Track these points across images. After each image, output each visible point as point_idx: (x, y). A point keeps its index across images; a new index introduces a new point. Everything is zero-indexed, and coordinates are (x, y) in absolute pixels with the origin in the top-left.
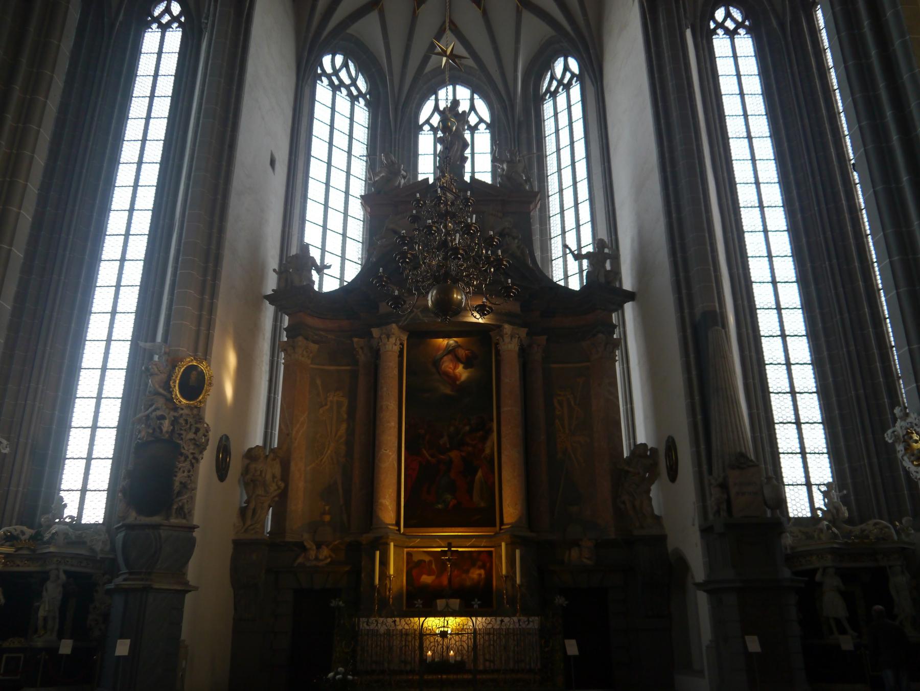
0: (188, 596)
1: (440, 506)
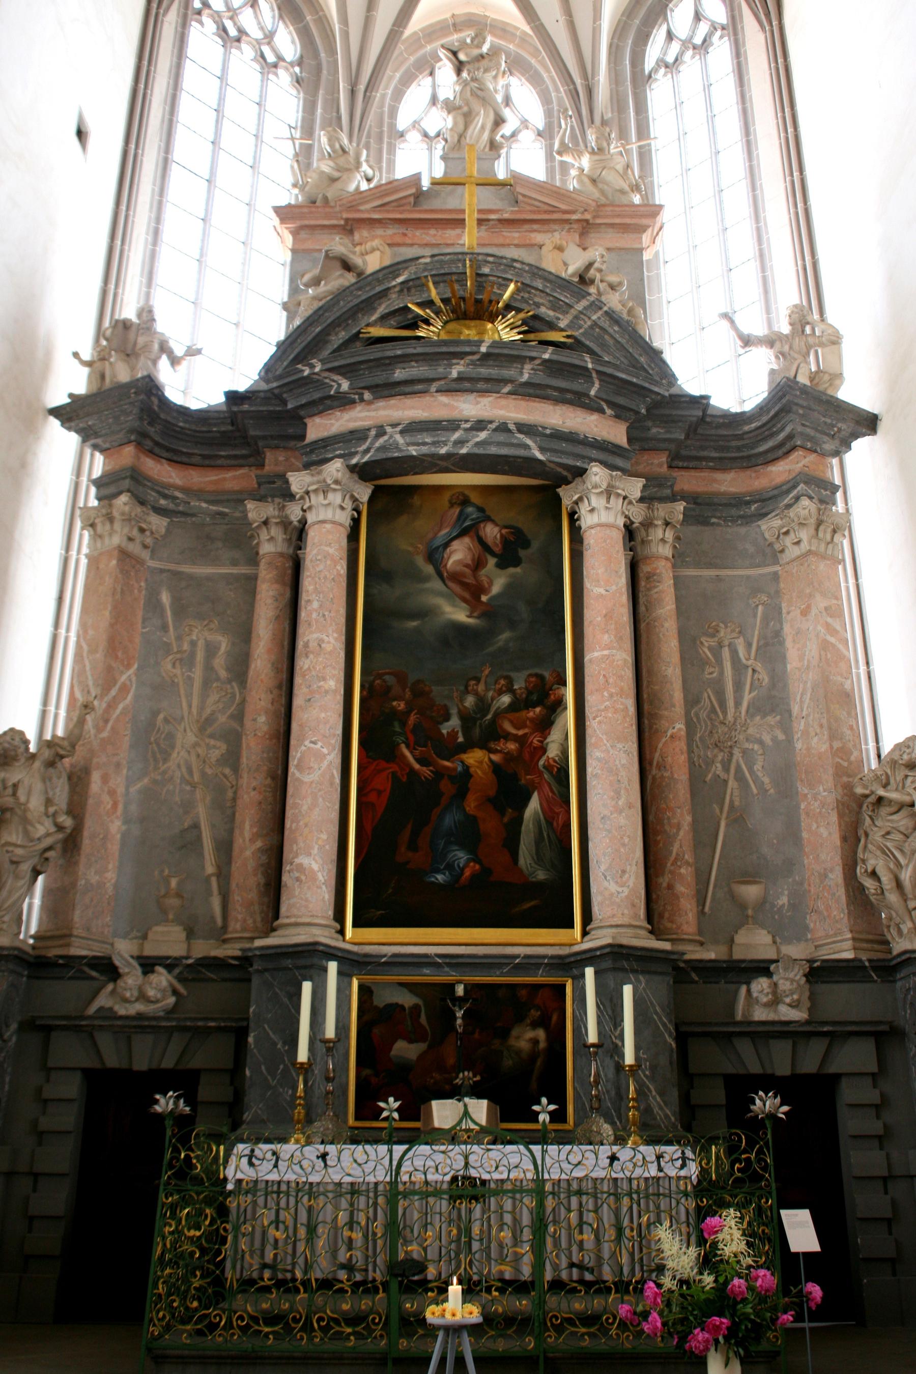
1: (440, 878)
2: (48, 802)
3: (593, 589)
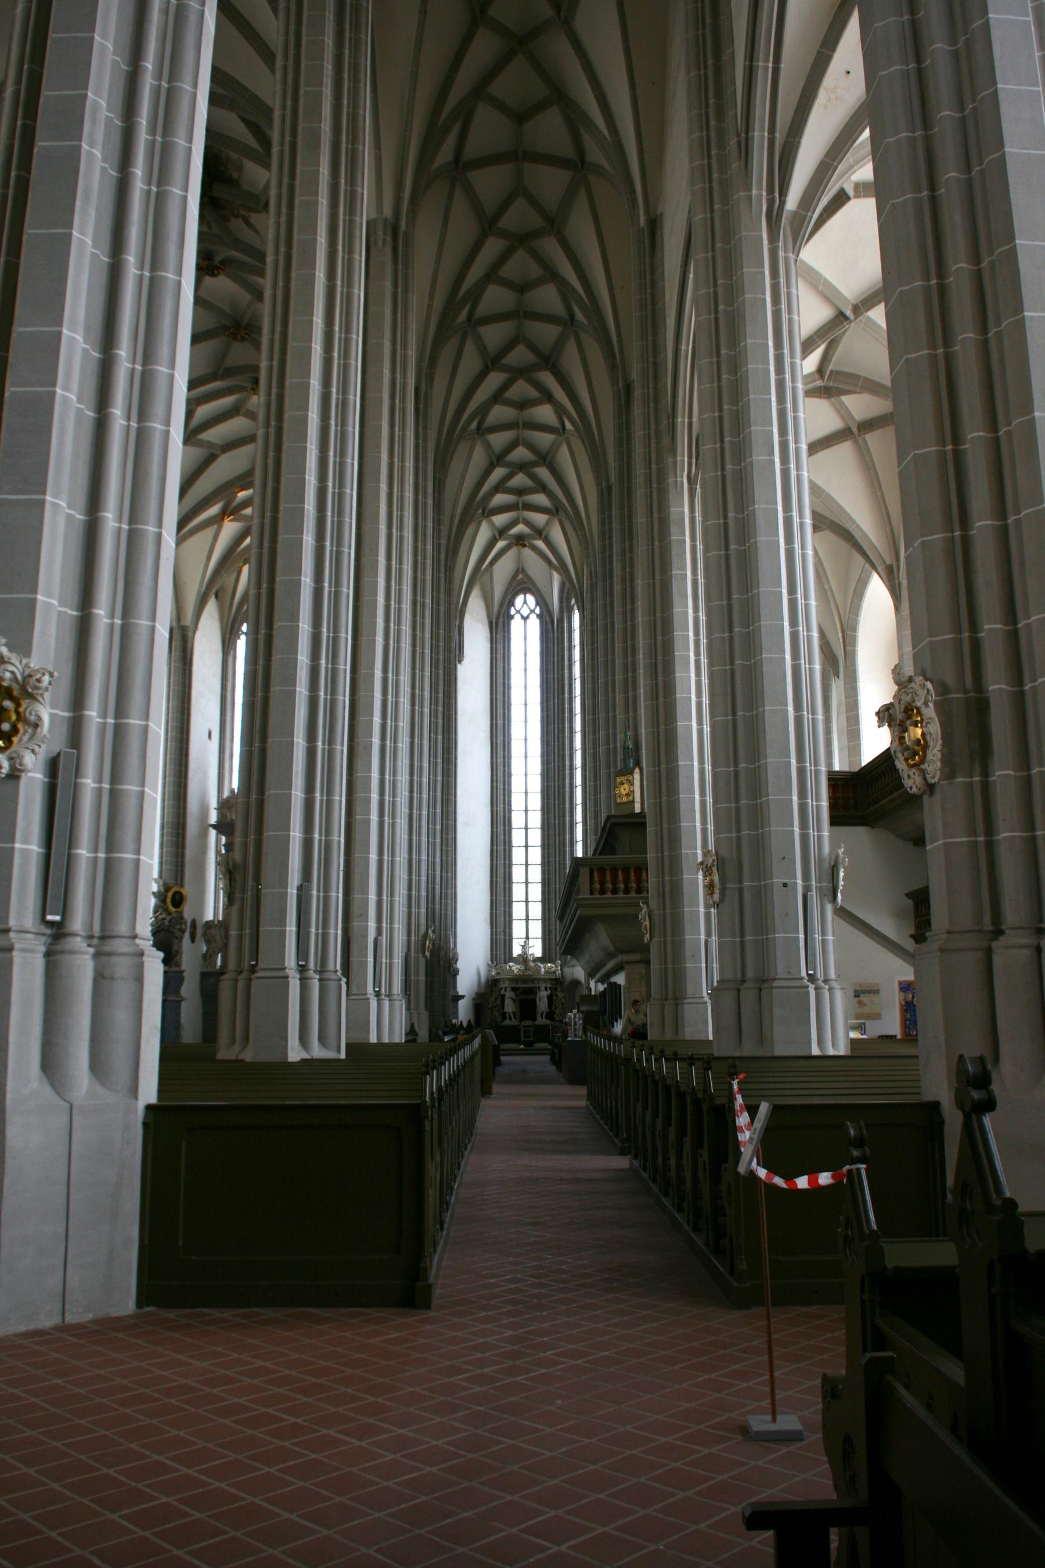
0: (183, 1004)
2: (221, 936)
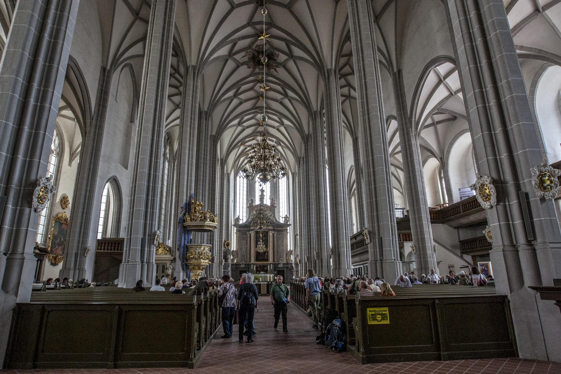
3: (270, 240)
